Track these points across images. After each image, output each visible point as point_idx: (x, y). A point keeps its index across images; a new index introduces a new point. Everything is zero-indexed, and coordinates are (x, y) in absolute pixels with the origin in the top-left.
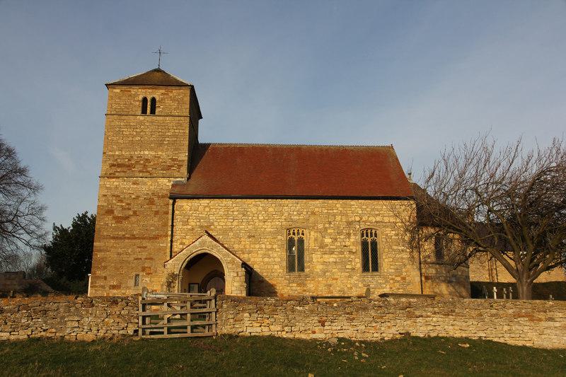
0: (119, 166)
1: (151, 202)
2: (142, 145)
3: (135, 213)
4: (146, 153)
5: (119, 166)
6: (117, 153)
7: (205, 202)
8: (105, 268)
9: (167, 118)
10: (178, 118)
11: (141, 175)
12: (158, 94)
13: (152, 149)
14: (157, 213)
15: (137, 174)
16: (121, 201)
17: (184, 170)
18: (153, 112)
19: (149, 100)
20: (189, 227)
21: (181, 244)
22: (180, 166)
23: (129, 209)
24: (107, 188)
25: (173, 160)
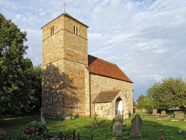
0: (69, 55)
1: (79, 74)
2: (75, 48)
3: (75, 77)
4: (77, 51)
5: (69, 55)
6: (68, 49)
7: (97, 76)
8: (68, 100)
9: (82, 38)
10: (84, 39)
11: (76, 61)
12: (79, 26)
13: (78, 50)
14: (81, 78)
15: (75, 60)
16: (71, 71)
17: (87, 61)
18: (77, 34)
19: (76, 27)
20: (94, 85)
21: (92, 92)
22: (86, 60)
23: (73, 75)
24: (66, 64)
25: (84, 57)
